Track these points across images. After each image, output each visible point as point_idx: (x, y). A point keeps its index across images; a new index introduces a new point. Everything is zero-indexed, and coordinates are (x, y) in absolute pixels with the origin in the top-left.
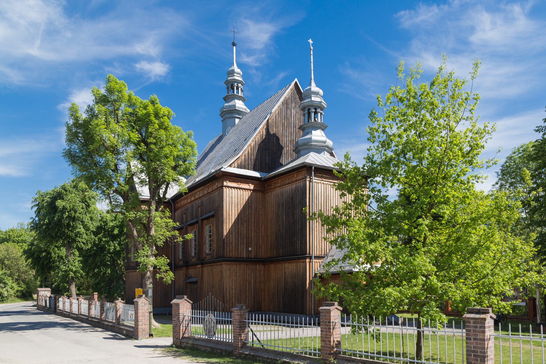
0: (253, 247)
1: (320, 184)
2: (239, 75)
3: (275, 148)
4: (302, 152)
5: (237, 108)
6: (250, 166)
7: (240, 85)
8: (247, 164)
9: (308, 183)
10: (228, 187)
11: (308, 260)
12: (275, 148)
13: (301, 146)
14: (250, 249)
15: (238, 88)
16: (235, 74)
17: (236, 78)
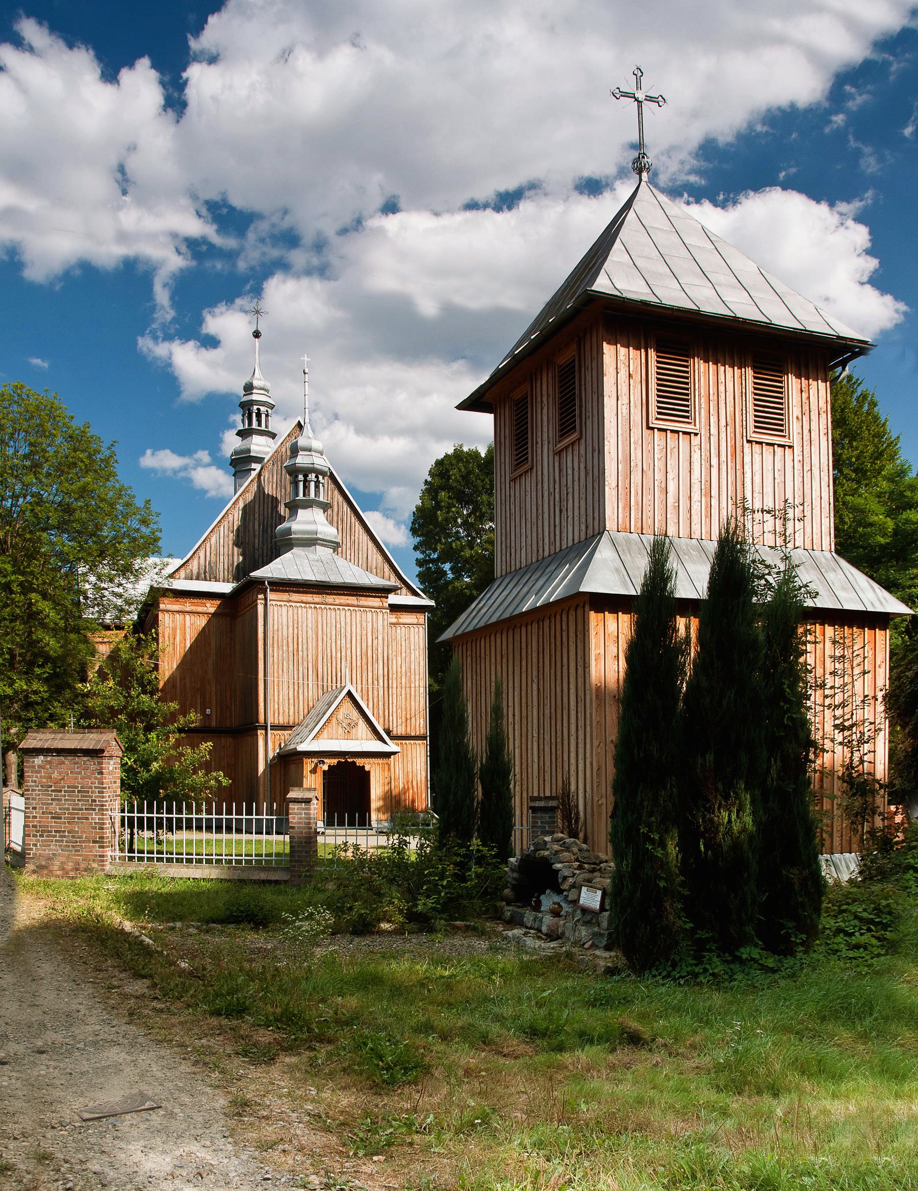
0: (214, 709)
1: (284, 609)
2: (262, 392)
3: (257, 541)
4: (282, 550)
5: (252, 454)
6: (207, 575)
7: (263, 409)
8: (202, 571)
9: (260, 608)
10: (168, 611)
11: (261, 733)
12: (257, 541)
13: (295, 534)
14: (208, 711)
15: (259, 415)
16: (255, 391)
17: (254, 397)
